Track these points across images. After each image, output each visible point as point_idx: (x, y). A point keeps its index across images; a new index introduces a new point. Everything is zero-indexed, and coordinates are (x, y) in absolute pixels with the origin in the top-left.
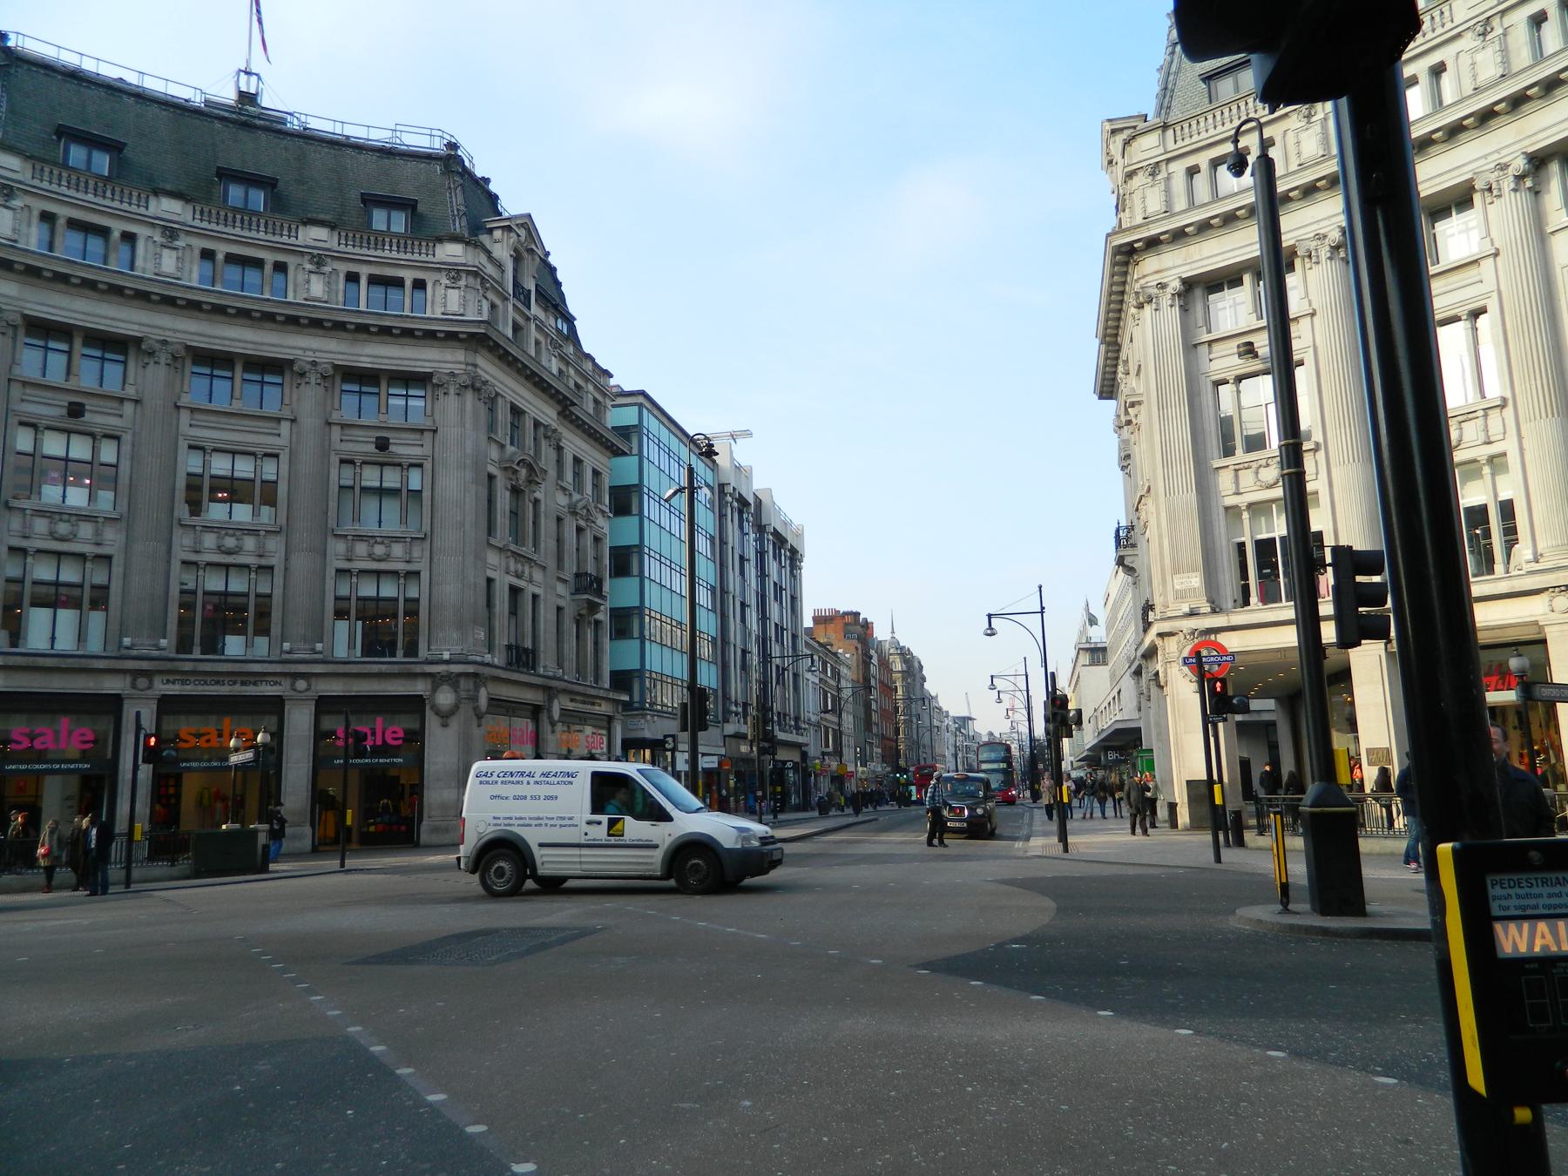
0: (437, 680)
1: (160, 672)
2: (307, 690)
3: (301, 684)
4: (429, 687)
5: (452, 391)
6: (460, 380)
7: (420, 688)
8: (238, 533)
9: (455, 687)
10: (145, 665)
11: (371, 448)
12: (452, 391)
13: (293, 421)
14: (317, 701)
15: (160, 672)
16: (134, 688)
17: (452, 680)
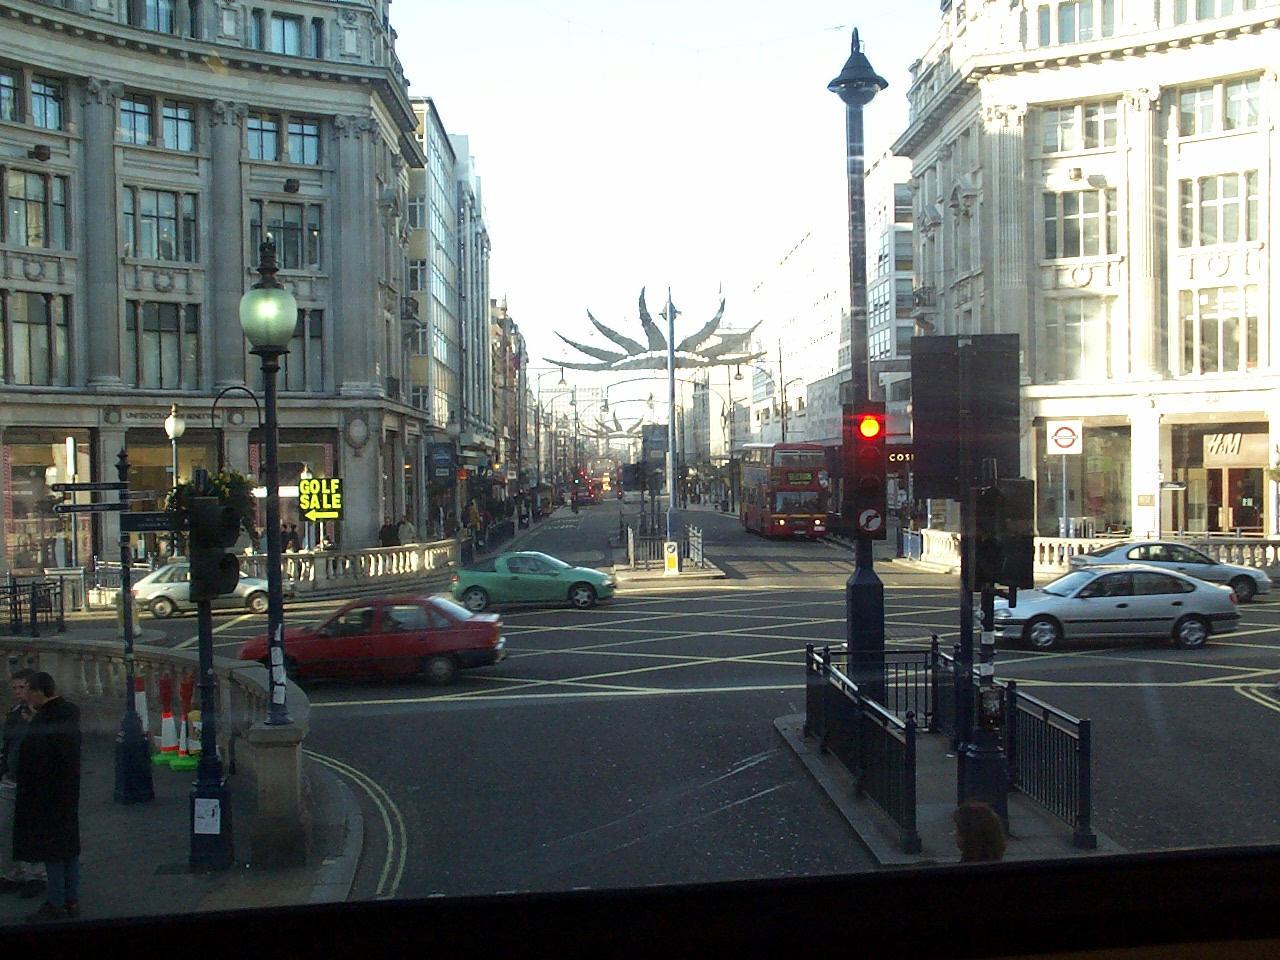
0: (350, 414)
1: (125, 406)
2: (243, 422)
3: (237, 418)
4: (342, 419)
5: (351, 134)
6: (360, 123)
7: (334, 420)
8: (171, 272)
9: (365, 420)
10: (116, 401)
11: (280, 189)
12: (351, 134)
13: (208, 160)
14: (250, 433)
15: (125, 406)
16: (107, 421)
17: (362, 413)
